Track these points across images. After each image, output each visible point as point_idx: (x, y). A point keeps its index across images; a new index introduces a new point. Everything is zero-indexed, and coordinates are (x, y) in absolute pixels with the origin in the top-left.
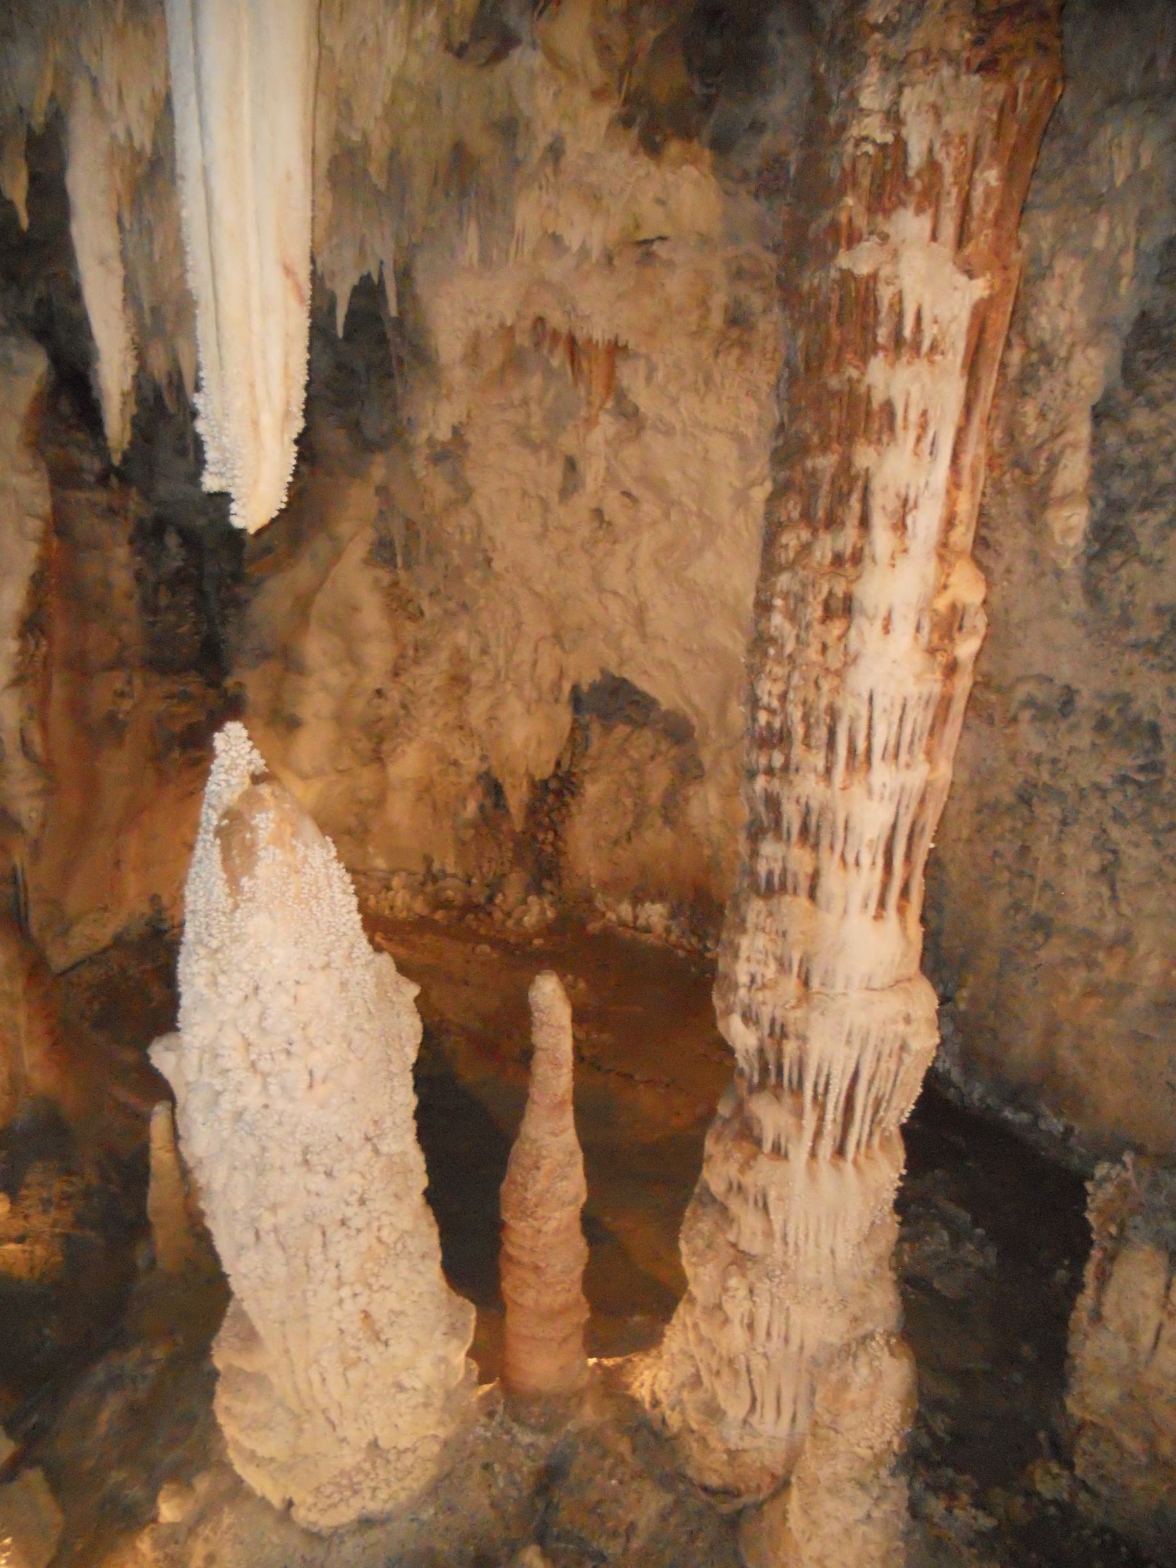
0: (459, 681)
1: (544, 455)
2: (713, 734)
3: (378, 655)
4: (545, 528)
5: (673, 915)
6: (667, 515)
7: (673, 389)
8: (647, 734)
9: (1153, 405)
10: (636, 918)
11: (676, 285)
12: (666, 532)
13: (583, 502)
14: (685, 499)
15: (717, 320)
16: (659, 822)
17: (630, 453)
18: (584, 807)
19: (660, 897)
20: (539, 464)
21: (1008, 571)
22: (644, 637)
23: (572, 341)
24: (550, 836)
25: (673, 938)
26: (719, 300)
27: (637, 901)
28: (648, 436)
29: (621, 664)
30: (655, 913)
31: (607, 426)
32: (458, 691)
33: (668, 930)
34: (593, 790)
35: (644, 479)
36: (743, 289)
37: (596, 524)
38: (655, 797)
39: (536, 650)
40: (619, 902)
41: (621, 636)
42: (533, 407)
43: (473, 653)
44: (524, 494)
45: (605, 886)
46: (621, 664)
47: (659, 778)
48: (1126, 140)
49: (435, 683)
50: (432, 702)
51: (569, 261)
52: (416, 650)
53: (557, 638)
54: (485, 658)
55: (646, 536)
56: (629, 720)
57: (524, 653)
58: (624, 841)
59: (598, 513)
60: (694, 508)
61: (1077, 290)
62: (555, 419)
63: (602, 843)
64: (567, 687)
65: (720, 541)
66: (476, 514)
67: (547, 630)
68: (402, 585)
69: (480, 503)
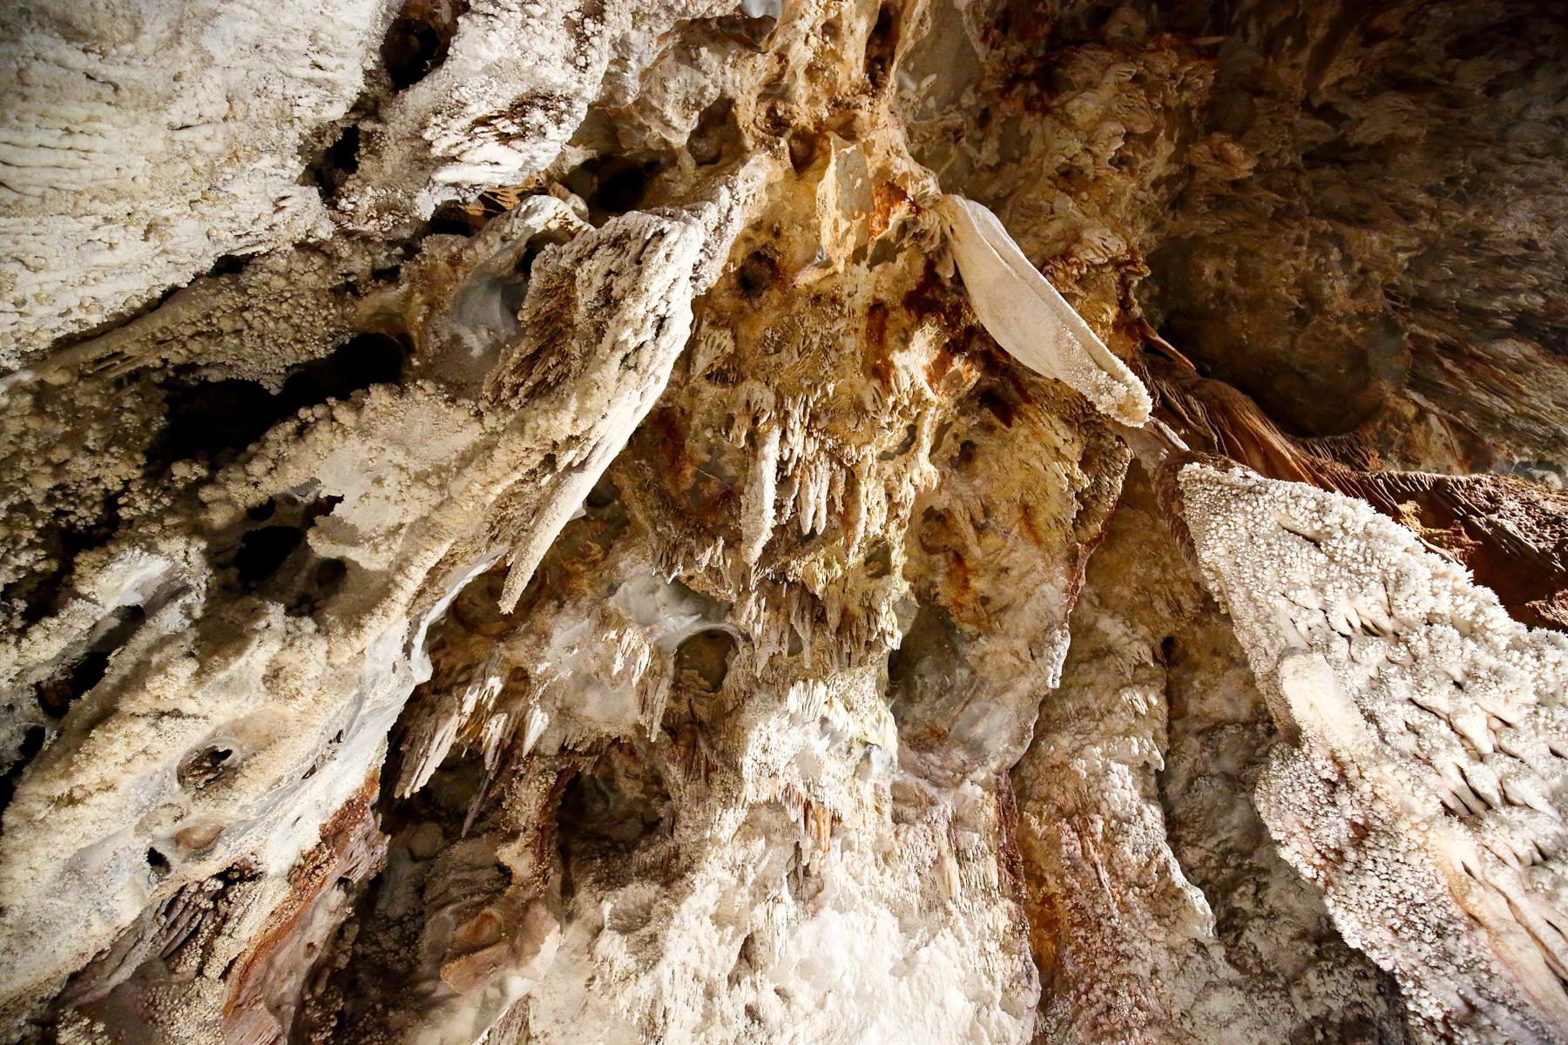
1: (731, 929)
4: (708, 1017)
6: (821, 1006)
7: (857, 867)
9: (1193, 844)
11: (867, 791)
12: (821, 1021)
14: (847, 980)
15: (888, 817)
17: (808, 930)
20: (721, 941)
21: (1154, 972)
23: (808, 806)
26: (887, 809)
28: (827, 913)
31: (787, 907)
35: (805, 969)
36: (901, 807)
42: (750, 868)
44: (696, 978)
48: (1139, 696)
51: (826, 741)
55: (801, 1027)
59: (751, 1012)
60: (853, 991)
61: (1129, 779)
62: (762, 889)
65: (883, 1018)
66: (657, 982)
69: (663, 969)
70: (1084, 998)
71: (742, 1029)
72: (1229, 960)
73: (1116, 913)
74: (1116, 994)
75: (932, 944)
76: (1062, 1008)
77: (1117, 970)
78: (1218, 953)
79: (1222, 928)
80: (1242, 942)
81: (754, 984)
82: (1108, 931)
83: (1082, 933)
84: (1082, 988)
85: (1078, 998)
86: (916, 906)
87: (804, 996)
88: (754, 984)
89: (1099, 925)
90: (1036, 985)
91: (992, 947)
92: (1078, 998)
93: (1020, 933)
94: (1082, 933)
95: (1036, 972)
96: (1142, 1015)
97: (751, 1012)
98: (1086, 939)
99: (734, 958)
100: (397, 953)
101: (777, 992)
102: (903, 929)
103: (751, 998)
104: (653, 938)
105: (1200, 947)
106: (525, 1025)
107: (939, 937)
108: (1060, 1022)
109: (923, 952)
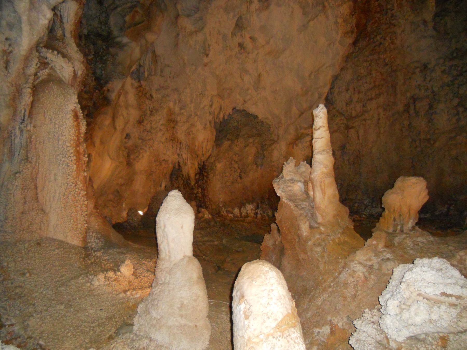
0: (172, 122)
2: (283, 122)
3: (134, 114)
5: (257, 208)
6: (268, 43)
8: (241, 140)
10: (241, 214)
13: (238, 39)
16: (254, 167)
18: (217, 172)
19: (249, 201)
21: (403, 31)
22: (257, 88)
24: (200, 190)
25: (259, 216)
27: (241, 205)
29: (245, 102)
30: (249, 208)
32: (172, 125)
33: (256, 214)
34: (219, 166)
37: (240, 48)
38: (250, 159)
39: (211, 101)
40: (233, 209)
41: (248, 89)
43: (177, 109)
45: (225, 205)
46: (245, 102)
47: (252, 151)
49: (161, 123)
50: (160, 130)
52: (151, 111)
53: (220, 96)
54: (183, 111)
56: (229, 140)
57: (206, 102)
58: (239, 179)
59: (241, 45)
63: (228, 184)
64: (221, 115)
67: (215, 93)
68: (144, 86)
70: (372, 40)
71: (237, 51)
72: (434, 28)
73: (396, 8)
74: (385, 39)
75: (316, 19)
76: (362, 44)
77: (389, 30)
78: (431, 25)
79: (436, 15)
80: (442, 21)
81: (241, 35)
82: (390, 15)
83: (379, 15)
84: (372, 36)
85: (369, 40)
86: (311, 4)
87: (261, 40)
88: (241, 35)
89: (387, 13)
90: (354, 35)
91: (340, 21)
92: (369, 40)
93: (353, 15)
94: (379, 15)
95: (356, 30)
96: (392, 46)
97: (241, 45)
98: (379, 18)
99: (234, 25)
100: (101, 28)
101: (251, 38)
102: (305, 14)
103: (240, 40)
104: (201, 19)
105: (425, 22)
106: (154, 52)
107: (319, 17)
108: (359, 49)
109: (311, 23)
